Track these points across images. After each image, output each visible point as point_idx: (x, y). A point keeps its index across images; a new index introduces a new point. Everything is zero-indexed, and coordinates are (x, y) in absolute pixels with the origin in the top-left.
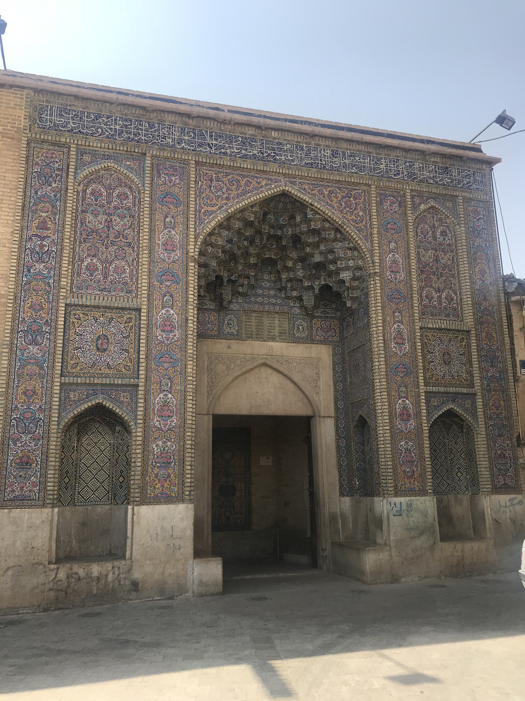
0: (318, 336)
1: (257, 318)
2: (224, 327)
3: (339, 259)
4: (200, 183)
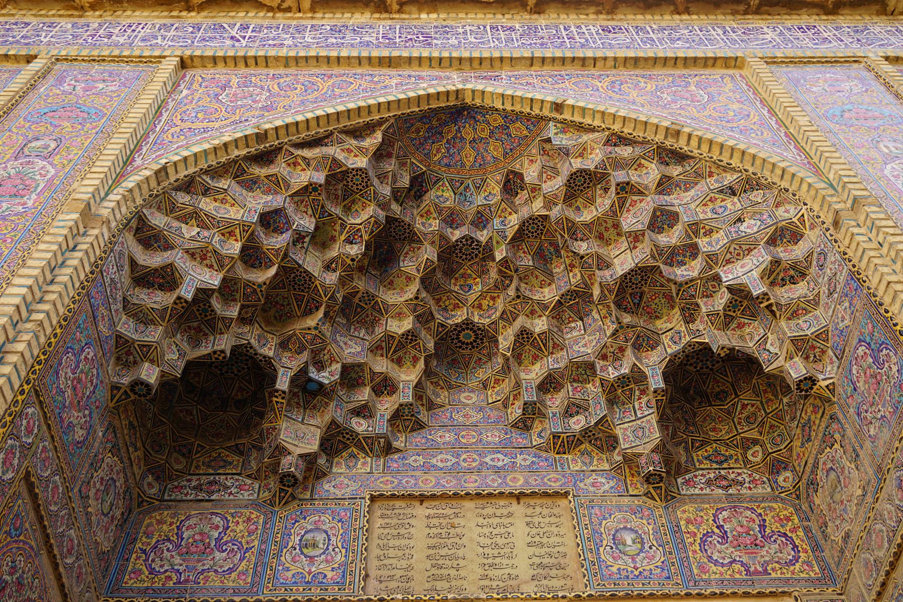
0: (716, 563)
1: (435, 521)
2: (286, 557)
3: (695, 228)
4: (185, 92)
